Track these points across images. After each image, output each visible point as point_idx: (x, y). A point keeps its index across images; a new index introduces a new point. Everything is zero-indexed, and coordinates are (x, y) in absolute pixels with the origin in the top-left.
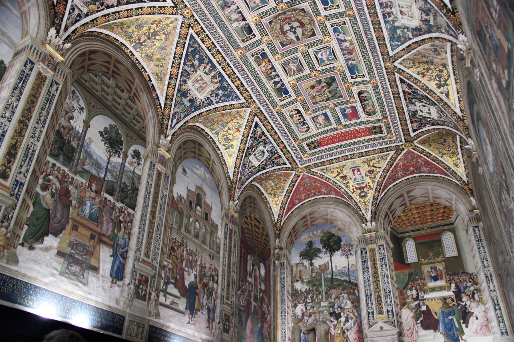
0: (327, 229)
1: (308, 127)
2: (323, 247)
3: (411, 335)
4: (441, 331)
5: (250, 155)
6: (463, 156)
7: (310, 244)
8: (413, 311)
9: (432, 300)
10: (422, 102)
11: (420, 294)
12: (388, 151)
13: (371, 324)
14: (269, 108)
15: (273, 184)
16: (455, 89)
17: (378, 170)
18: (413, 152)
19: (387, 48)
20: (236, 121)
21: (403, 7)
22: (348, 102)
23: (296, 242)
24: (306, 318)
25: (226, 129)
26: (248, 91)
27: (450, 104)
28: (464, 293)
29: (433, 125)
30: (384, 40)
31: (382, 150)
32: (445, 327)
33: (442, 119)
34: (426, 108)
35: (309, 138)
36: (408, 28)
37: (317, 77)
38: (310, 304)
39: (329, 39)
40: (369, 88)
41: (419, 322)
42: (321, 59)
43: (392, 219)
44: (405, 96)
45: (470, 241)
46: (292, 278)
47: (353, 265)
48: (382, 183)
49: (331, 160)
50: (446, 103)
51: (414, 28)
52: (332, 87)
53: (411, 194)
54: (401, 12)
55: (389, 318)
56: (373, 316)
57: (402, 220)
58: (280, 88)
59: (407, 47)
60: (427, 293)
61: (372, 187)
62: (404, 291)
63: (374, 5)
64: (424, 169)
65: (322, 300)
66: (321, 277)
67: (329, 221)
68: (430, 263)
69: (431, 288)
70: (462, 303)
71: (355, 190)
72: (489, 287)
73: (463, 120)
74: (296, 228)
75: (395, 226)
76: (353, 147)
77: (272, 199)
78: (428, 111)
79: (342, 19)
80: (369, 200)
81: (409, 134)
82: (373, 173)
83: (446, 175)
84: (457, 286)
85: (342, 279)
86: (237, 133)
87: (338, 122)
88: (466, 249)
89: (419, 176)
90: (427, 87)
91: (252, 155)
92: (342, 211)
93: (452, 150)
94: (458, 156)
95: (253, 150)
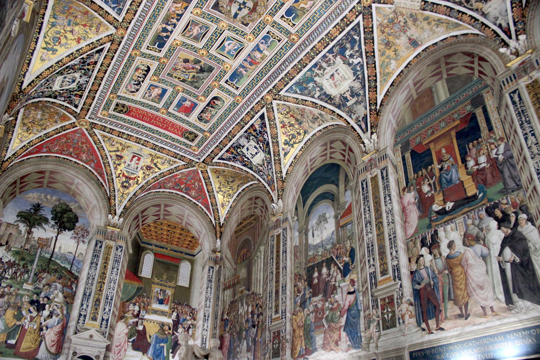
0: (65, 199)
1: (137, 90)
3: (119, 353)
4: (149, 356)
5: (62, 74)
6: (234, 202)
7: (37, 207)
8: (129, 327)
9: (150, 322)
10: (258, 144)
11: (141, 312)
12: (180, 159)
13: (78, 328)
14: (130, 46)
15: (39, 117)
16: (295, 154)
17: (157, 170)
18: (198, 174)
19: (284, 87)
20: (88, 30)
21: (338, 74)
22: (197, 97)
23: (18, 196)
25: (69, 29)
26: (135, 15)
27: (282, 163)
28: (182, 324)
29: (245, 165)
30: (291, 80)
31: (175, 156)
32: (154, 352)
33: (261, 168)
34: (256, 150)
35: (128, 100)
36: (322, 89)
37: (202, 57)
38: (8, 281)
39: (252, 39)
40: (228, 100)
41: (131, 340)
42: (224, 47)
43: (141, 224)
44: (249, 128)
45: (203, 278)
47: (81, 254)
49: (123, 133)
50: (280, 160)
51: (327, 93)
52: (201, 75)
53: (168, 209)
54: (332, 75)
56: (84, 321)
57: (150, 230)
58: (162, 37)
59: (302, 100)
60: (149, 313)
61: (139, 183)
62: (127, 304)
63: (320, 52)
64: (193, 193)
65: (26, 281)
66: (36, 252)
67: (72, 192)
68: (161, 285)
69: (154, 310)
70: (176, 334)
71: (121, 175)
72: (204, 325)
73: (283, 182)
74: (25, 179)
76: (155, 136)
77: (20, 131)
78: (254, 153)
79: (282, 36)
80: (129, 193)
81: (214, 158)
82: (150, 170)
83: (208, 209)
84: (178, 316)
85: (63, 265)
86: (74, 43)
87: (167, 105)
88: (197, 284)
89: (182, 196)
90: (277, 137)
91: (63, 76)
92: (90, 188)
93: (231, 192)
94: (230, 200)
95: (69, 72)
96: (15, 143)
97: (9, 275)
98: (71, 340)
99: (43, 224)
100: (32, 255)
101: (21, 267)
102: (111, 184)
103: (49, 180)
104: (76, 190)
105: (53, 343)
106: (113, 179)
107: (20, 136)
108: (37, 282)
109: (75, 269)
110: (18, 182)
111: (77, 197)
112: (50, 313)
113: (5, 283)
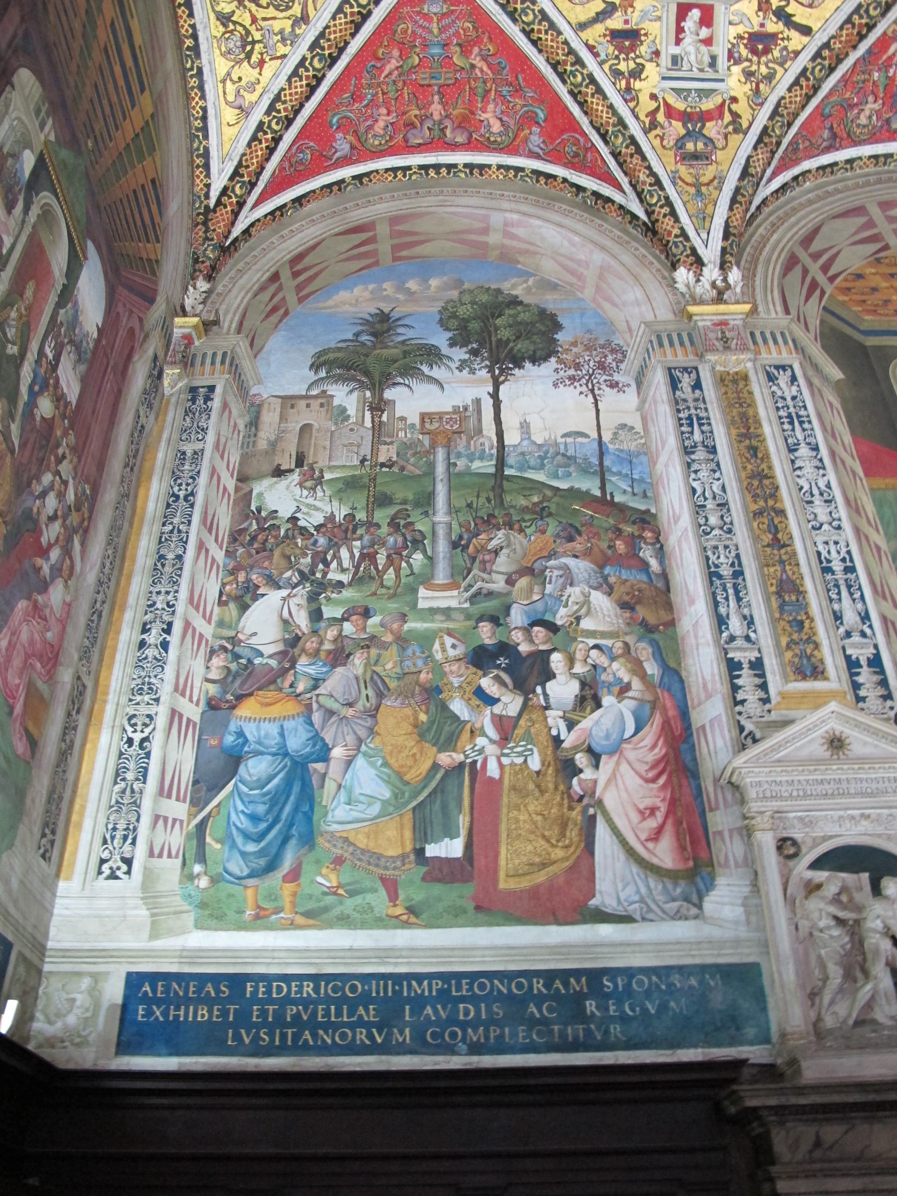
2: (453, 343)
13: (749, 726)
17: (796, 40)
23: (296, 309)
24: (304, 665)
38: (347, 593)
43: (821, 279)
46: (245, 458)
47: (623, 426)
48: (796, 115)
55: (859, 699)
56: (764, 687)
57: (874, 290)
61: (745, 125)
65: (426, 579)
66: (432, 466)
67: (497, 253)
71: (661, 117)
74: (307, 261)
75: (843, 303)
77: (222, 66)
82: (766, 51)
85: (564, 485)
92: (560, 225)
96: (225, 128)
97: (343, 570)
98: (735, 787)
99: (425, 369)
100: (413, 478)
101: (385, 529)
102: (636, 160)
103: (396, 241)
104: (507, 242)
105: (652, 823)
106: (633, 141)
107: (228, 82)
108: (475, 571)
109: (624, 486)
110: (286, 274)
111: (521, 259)
112: (583, 684)
113: (338, 603)
